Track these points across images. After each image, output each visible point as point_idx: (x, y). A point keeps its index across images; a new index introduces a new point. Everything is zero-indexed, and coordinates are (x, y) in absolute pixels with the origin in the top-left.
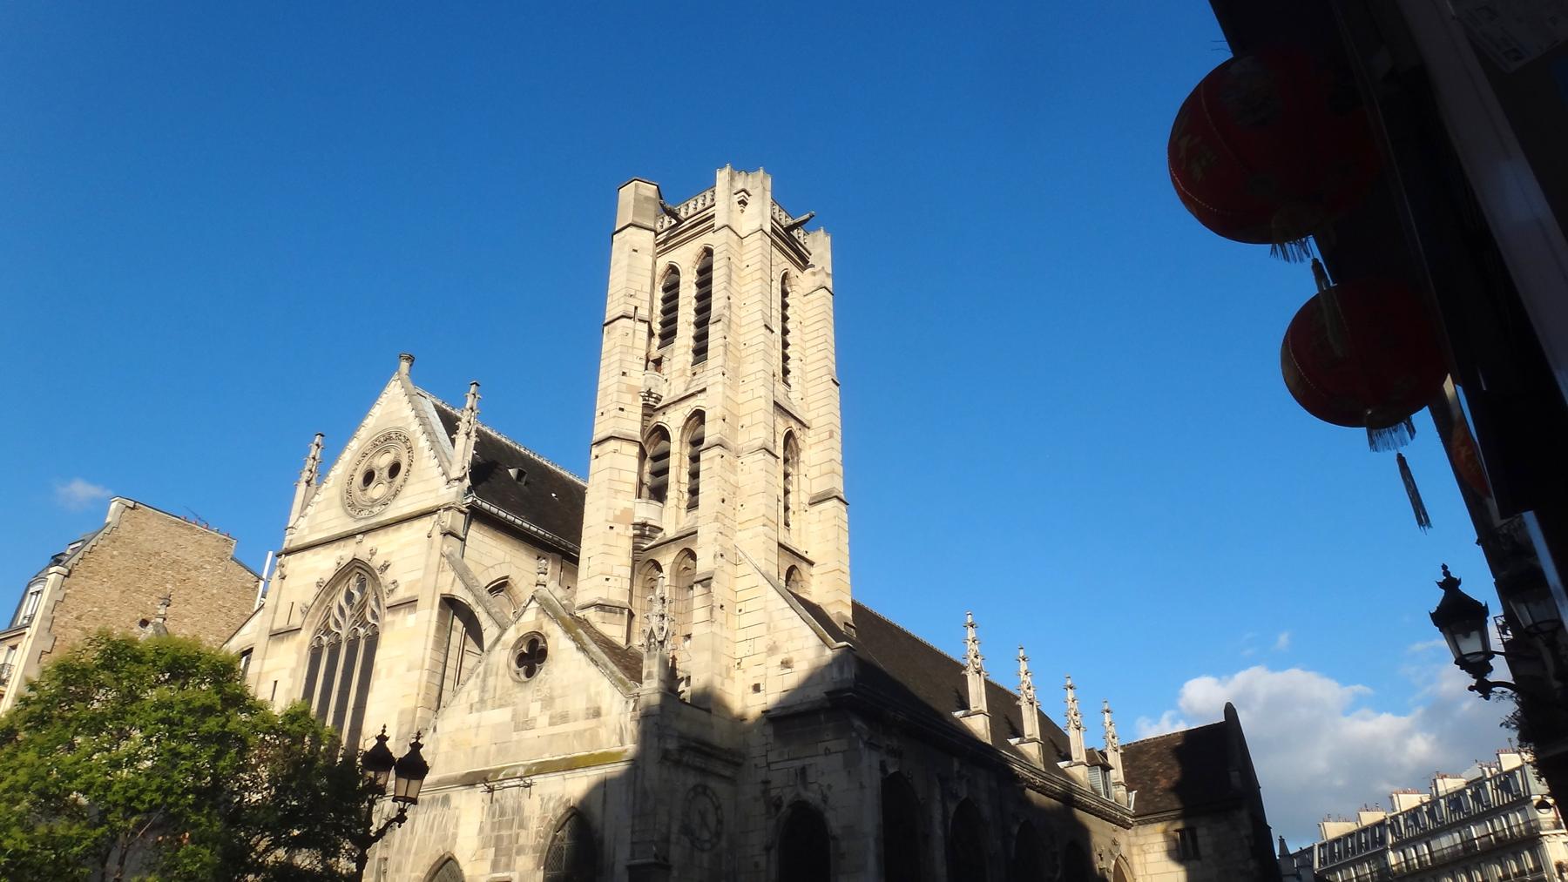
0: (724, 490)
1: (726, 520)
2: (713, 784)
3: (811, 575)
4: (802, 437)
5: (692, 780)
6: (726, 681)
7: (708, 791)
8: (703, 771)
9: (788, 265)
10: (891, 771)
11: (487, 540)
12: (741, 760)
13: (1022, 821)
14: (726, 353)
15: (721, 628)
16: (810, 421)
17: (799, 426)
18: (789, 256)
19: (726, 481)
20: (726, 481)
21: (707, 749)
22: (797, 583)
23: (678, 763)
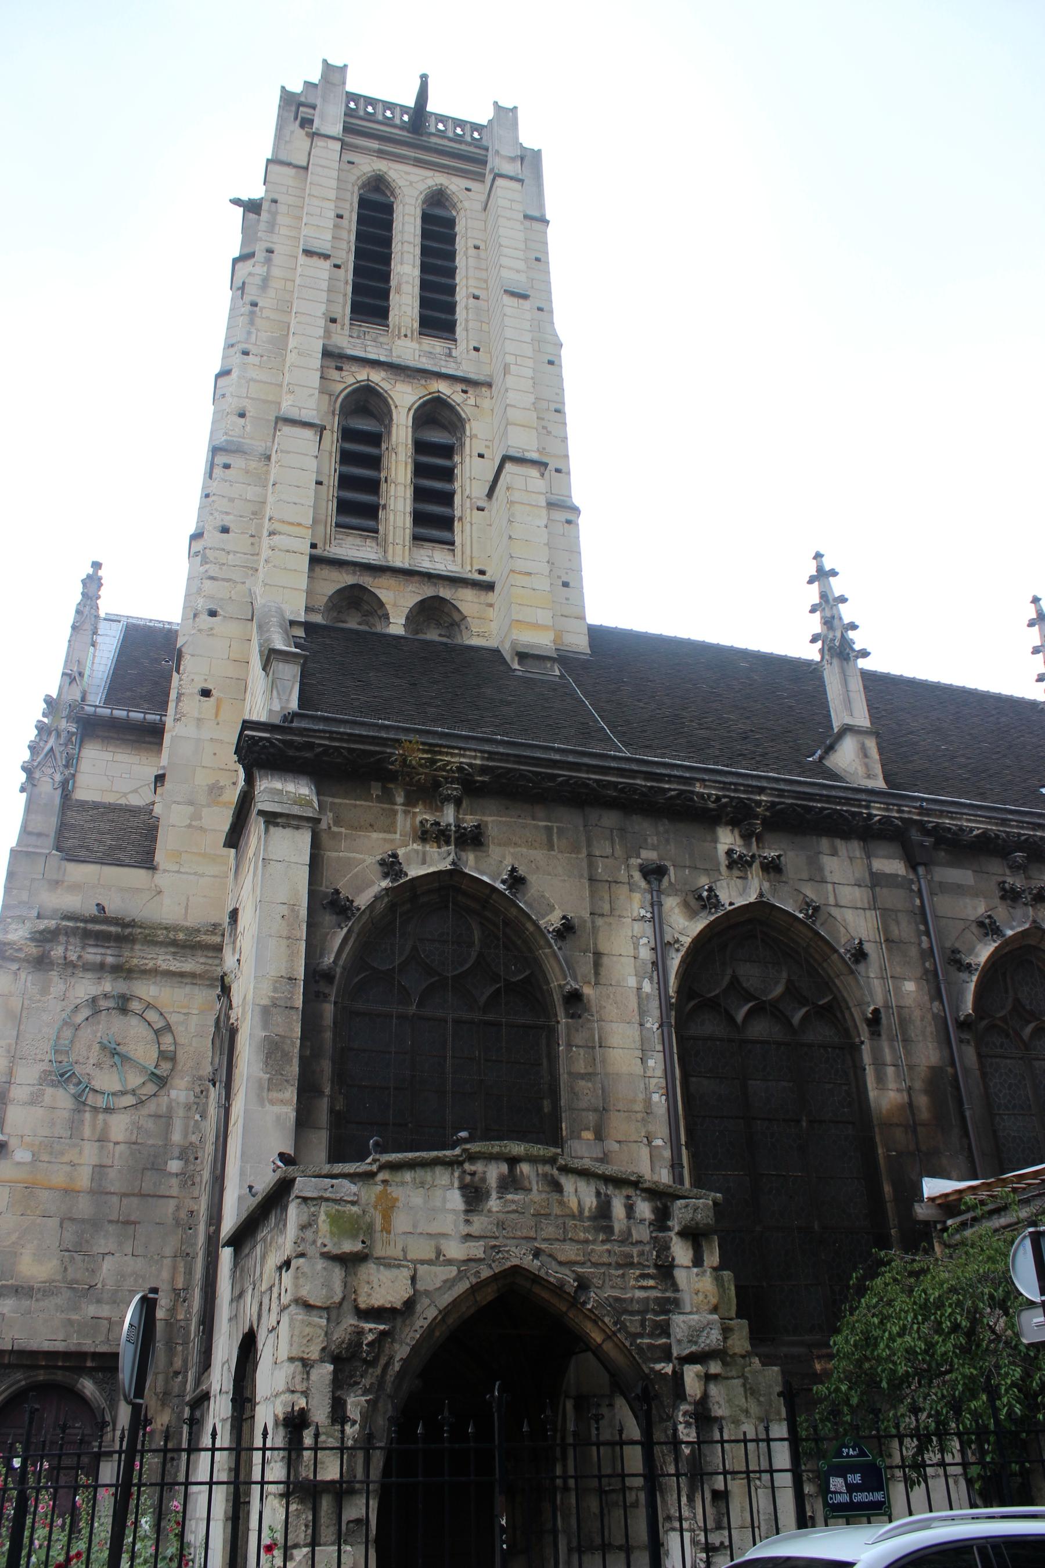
0: (227, 513)
1: (231, 556)
2: (147, 990)
3: (491, 605)
4: (472, 401)
5: (85, 988)
6: (205, 812)
7: (135, 1006)
8: (121, 971)
9: (435, 179)
10: (414, 871)
11: (119, 757)
12: (218, 939)
13: (1010, 933)
14: (252, 323)
15: (198, 727)
16: (491, 376)
17: (459, 387)
18: (444, 166)
19: (232, 500)
20: (232, 500)
21: (113, 929)
22: (459, 626)
23: (41, 963)
